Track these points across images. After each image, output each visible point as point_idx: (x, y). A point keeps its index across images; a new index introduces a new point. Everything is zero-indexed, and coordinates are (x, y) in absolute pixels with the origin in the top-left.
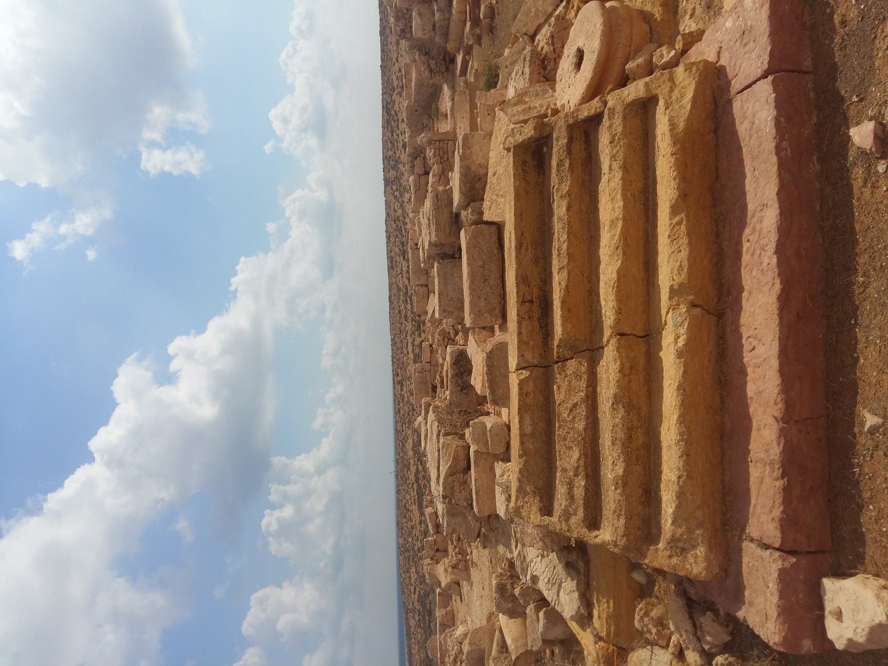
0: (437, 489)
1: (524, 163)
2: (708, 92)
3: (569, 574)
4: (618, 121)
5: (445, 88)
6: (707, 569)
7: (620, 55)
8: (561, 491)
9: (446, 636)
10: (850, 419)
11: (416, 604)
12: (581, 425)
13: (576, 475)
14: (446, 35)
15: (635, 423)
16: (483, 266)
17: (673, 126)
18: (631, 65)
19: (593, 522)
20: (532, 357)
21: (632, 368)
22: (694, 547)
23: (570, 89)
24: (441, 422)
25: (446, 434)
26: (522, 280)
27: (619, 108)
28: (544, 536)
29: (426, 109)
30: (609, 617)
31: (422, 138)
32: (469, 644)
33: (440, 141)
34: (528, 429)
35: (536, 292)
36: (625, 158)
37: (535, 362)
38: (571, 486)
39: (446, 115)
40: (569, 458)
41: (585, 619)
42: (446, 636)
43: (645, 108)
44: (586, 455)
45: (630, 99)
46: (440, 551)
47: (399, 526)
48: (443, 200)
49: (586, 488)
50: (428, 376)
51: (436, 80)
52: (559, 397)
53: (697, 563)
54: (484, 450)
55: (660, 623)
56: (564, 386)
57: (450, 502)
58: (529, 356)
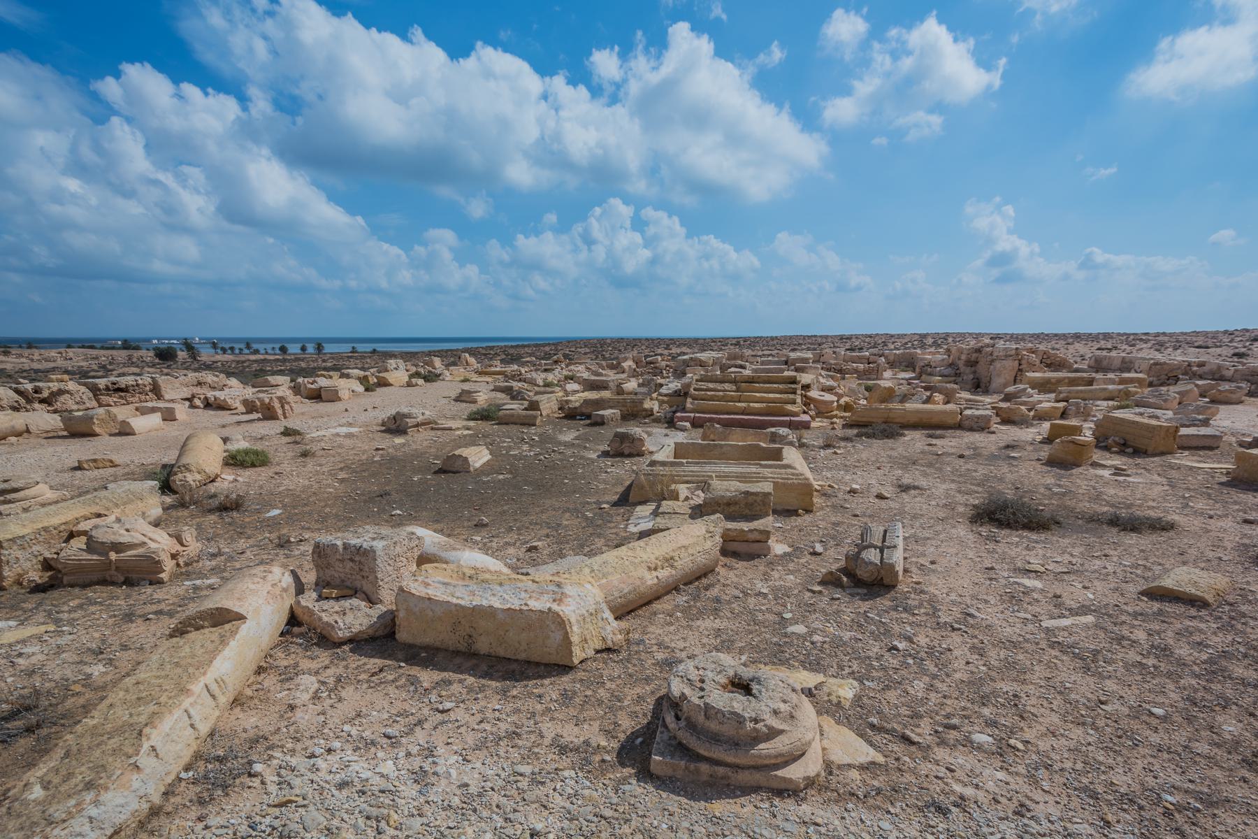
14: (930, 374)
23: (814, 394)
40: (711, 385)
43: (794, 402)
47: (620, 340)
53: (689, 405)
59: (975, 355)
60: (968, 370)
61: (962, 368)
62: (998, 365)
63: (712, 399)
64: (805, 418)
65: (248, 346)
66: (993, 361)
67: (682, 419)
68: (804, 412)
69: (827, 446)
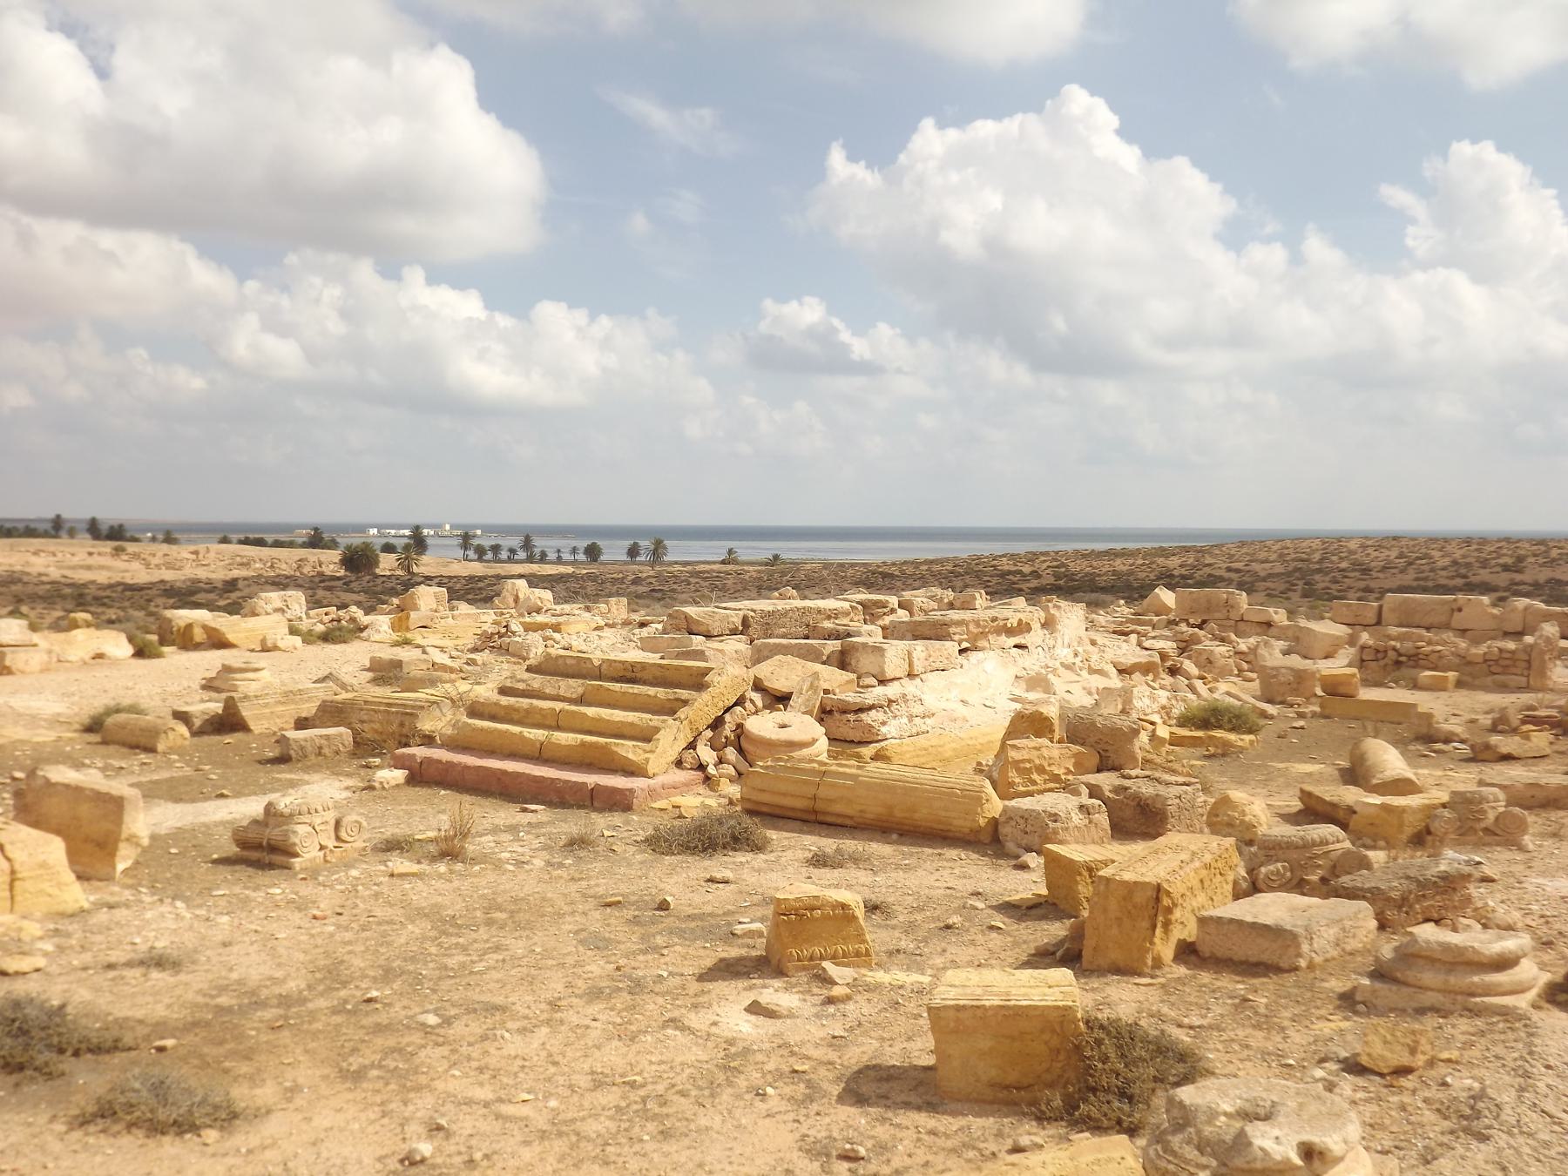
11: (1207, 570)
33: (1529, 662)
40: (537, 681)
50: (1217, 615)
52: (571, 681)
65: (466, 541)
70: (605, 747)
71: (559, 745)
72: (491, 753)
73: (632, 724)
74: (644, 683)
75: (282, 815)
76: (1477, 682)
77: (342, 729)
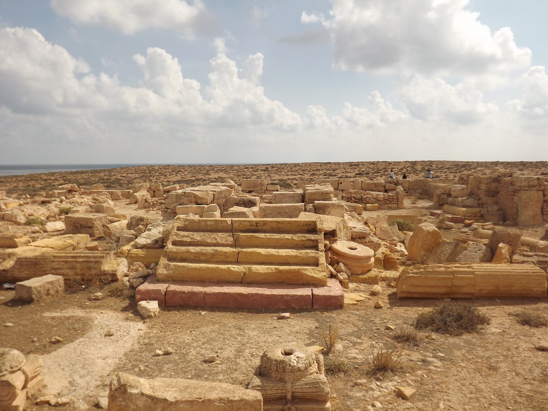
0: (188, 190)
1: (310, 225)
2: (316, 282)
3: (153, 241)
4: (313, 255)
5: (431, 204)
6: (160, 274)
7: (348, 262)
8: (186, 233)
9: (107, 195)
10: (204, 310)
11: (115, 177)
12: (209, 241)
13: (191, 238)
14: (452, 204)
15: (208, 257)
16: (285, 212)
17: (305, 269)
18: (341, 265)
19: (174, 243)
20: (236, 225)
21: (227, 256)
22: (167, 271)
24: (220, 193)
25: (214, 195)
26: (265, 223)
27: (317, 255)
28: (168, 231)
29: (424, 191)
30: (137, 254)
31: (400, 188)
32: (107, 207)
33: (397, 199)
34: (208, 223)
35: (260, 228)
36: (299, 257)
37: (234, 227)
38: (186, 236)
39: (414, 204)
40: (197, 236)
41: (136, 247)
42: (107, 195)
43: (317, 264)
44: (198, 242)
45: (320, 259)
46: (154, 192)
47: (167, 167)
48: (325, 196)
49: (186, 242)
51: (435, 198)
52: (219, 234)
53: (161, 271)
54: (205, 211)
55: (137, 270)
56: (224, 236)
57: (182, 195)
58: (236, 224)
59: (494, 185)
60: (490, 200)
61: (485, 199)
62: (524, 195)
63: (197, 258)
64: (333, 288)
66: (515, 192)
67: (149, 296)
68: (332, 276)
69: (381, 369)
70: (298, 272)
71: (260, 273)
72: (203, 282)
73: (296, 256)
74: (265, 232)
75: (299, 370)
76: (382, 207)
77: (50, 278)
